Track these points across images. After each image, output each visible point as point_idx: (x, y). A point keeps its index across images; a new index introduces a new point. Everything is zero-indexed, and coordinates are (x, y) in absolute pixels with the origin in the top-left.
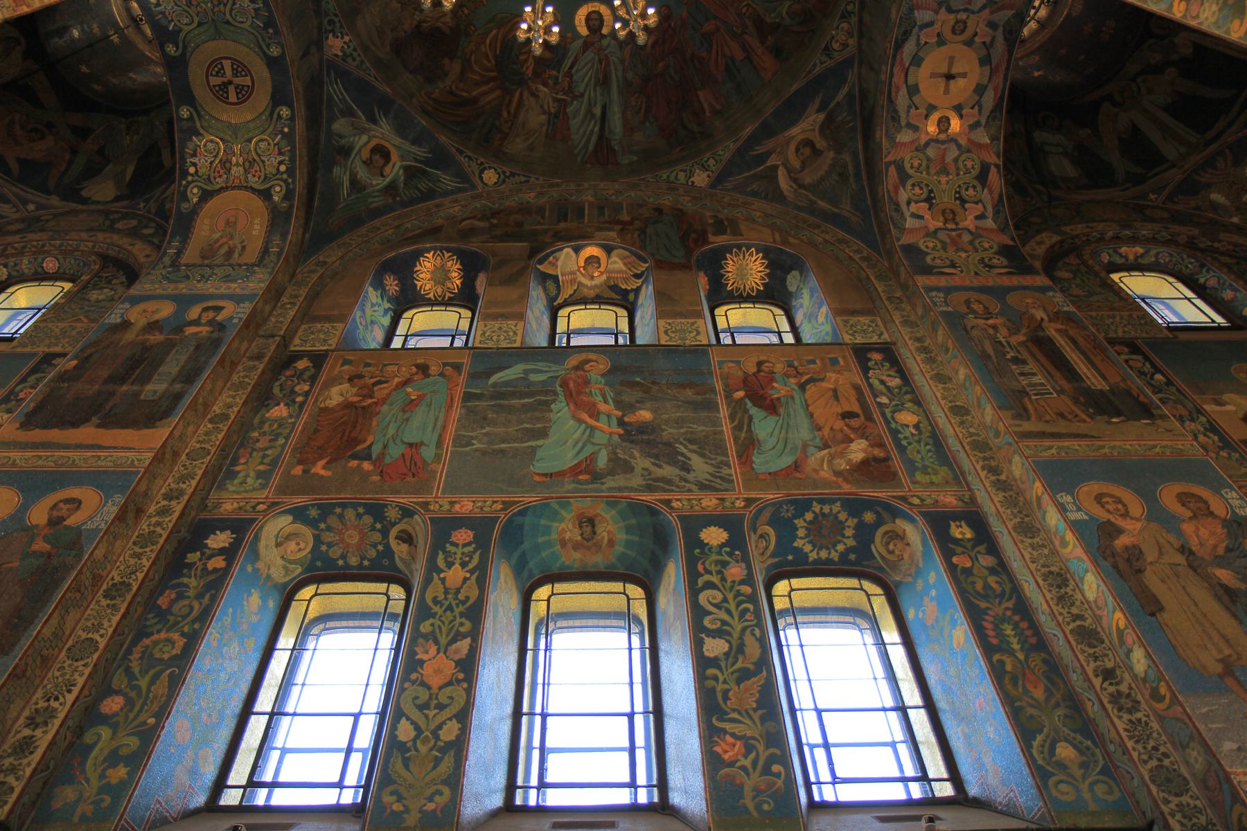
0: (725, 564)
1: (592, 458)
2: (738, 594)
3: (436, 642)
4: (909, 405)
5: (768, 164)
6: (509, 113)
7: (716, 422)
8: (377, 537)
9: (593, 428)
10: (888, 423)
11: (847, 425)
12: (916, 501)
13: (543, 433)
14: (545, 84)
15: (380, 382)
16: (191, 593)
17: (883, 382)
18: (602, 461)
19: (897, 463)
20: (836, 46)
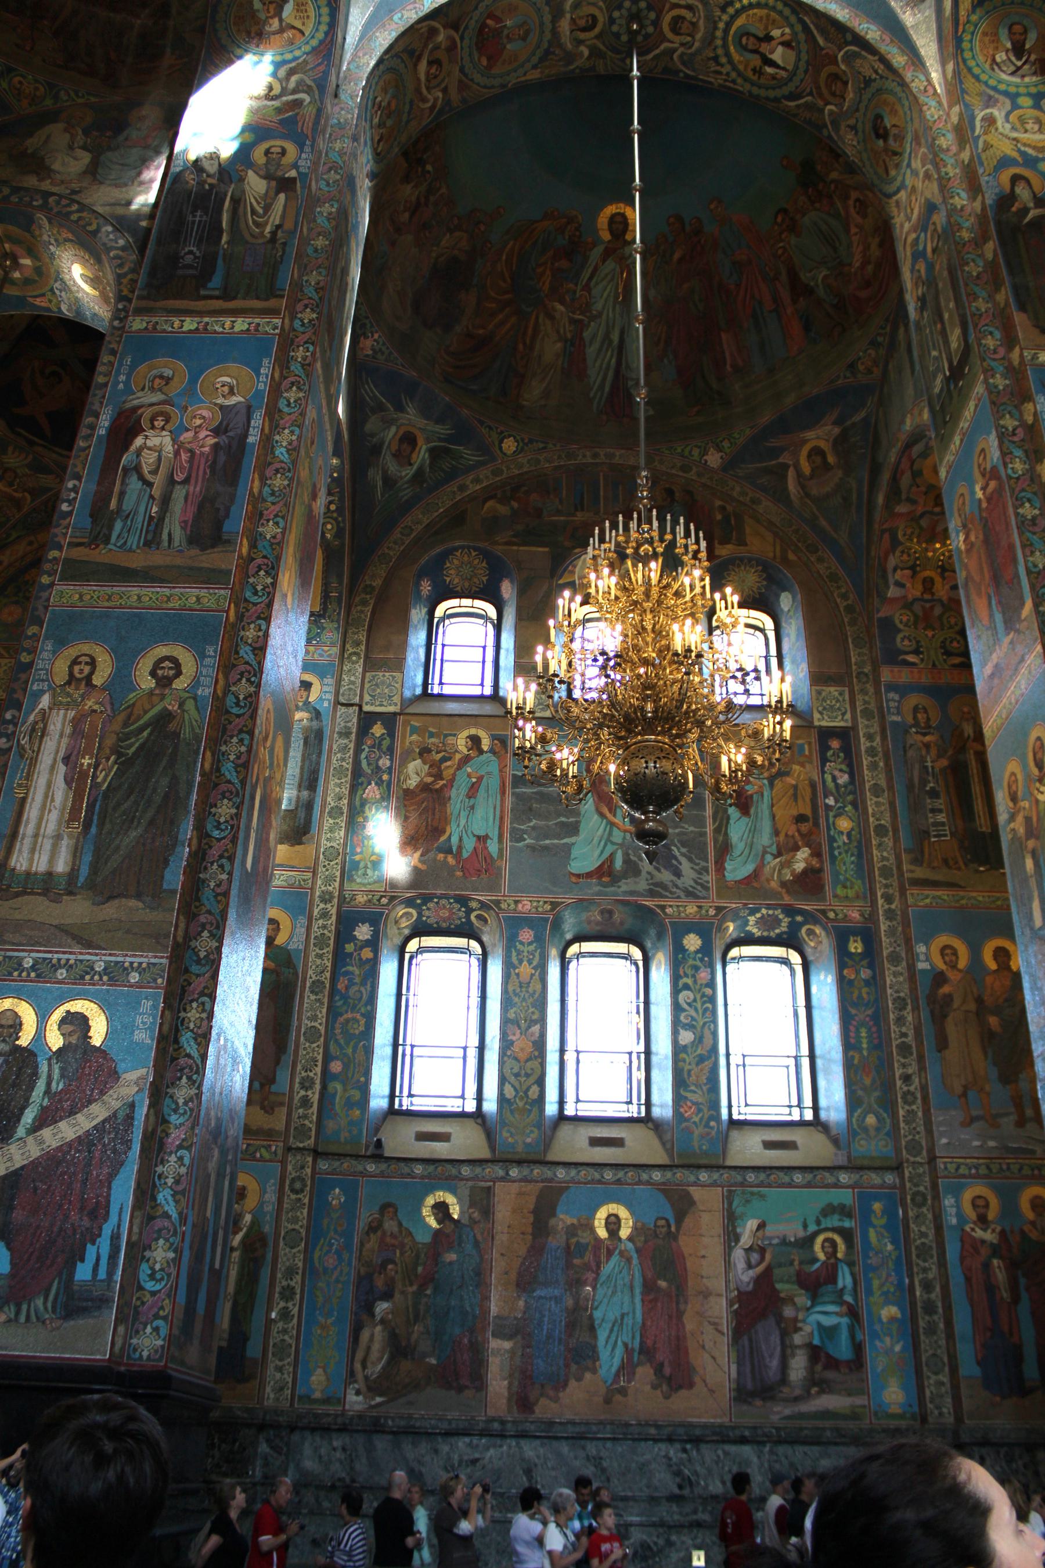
0: (696, 968)
1: (611, 858)
2: (703, 995)
3: (519, 1027)
4: (849, 808)
5: (781, 460)
6: (524, 344)
7: (701, 822)
8: (462, 914)
9: (612, 824)
10: (829, 829)
11: (798, 831)
12: (831, 915)
13: (573, 829)
14: (562, 302)
15: (444, 759)
16: (357, 980)
17: (834, 779)
18: (618, 863)
19: (827, 877)
20: (861, 368)
